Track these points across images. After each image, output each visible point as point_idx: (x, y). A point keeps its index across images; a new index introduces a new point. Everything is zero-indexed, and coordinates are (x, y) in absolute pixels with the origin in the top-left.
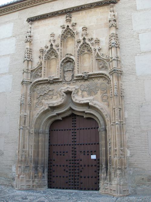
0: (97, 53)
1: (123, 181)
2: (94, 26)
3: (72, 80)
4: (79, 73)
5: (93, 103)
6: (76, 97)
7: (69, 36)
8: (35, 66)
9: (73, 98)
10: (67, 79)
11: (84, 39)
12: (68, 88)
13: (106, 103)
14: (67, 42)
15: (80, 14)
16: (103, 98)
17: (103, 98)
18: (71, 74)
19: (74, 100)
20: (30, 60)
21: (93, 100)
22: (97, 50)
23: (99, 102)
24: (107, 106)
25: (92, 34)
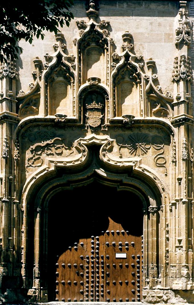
0: (151, 85)
1: (191, 284)
2: (146, 35)
3: (101, 125)
4: (115, 116)
5: (140, 168)
6: (109, 156)
7: (93, 45)
8: (25, 90)
9: (101, 156)
10: (90, 122)
11: (127, 56)
12: (93, 138)
13: (161, 169)
14: (89, 54)
15: (116, 6)
16: (156, 161)
17: (156, 161)
18: (99, 116)
19: (105, 160)
20: (15, 77)
21: (140, 162)
22: (151, 81)
23: (149, 166)
24: (164, 175)
25: (141, 49)
